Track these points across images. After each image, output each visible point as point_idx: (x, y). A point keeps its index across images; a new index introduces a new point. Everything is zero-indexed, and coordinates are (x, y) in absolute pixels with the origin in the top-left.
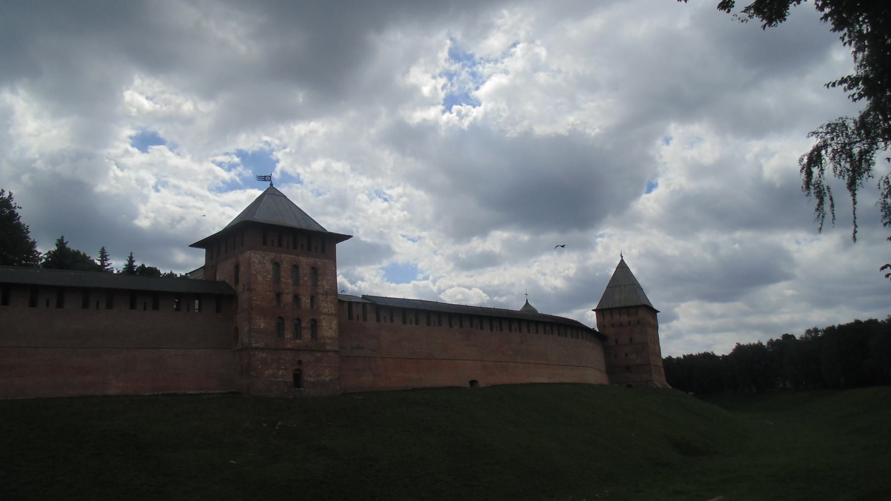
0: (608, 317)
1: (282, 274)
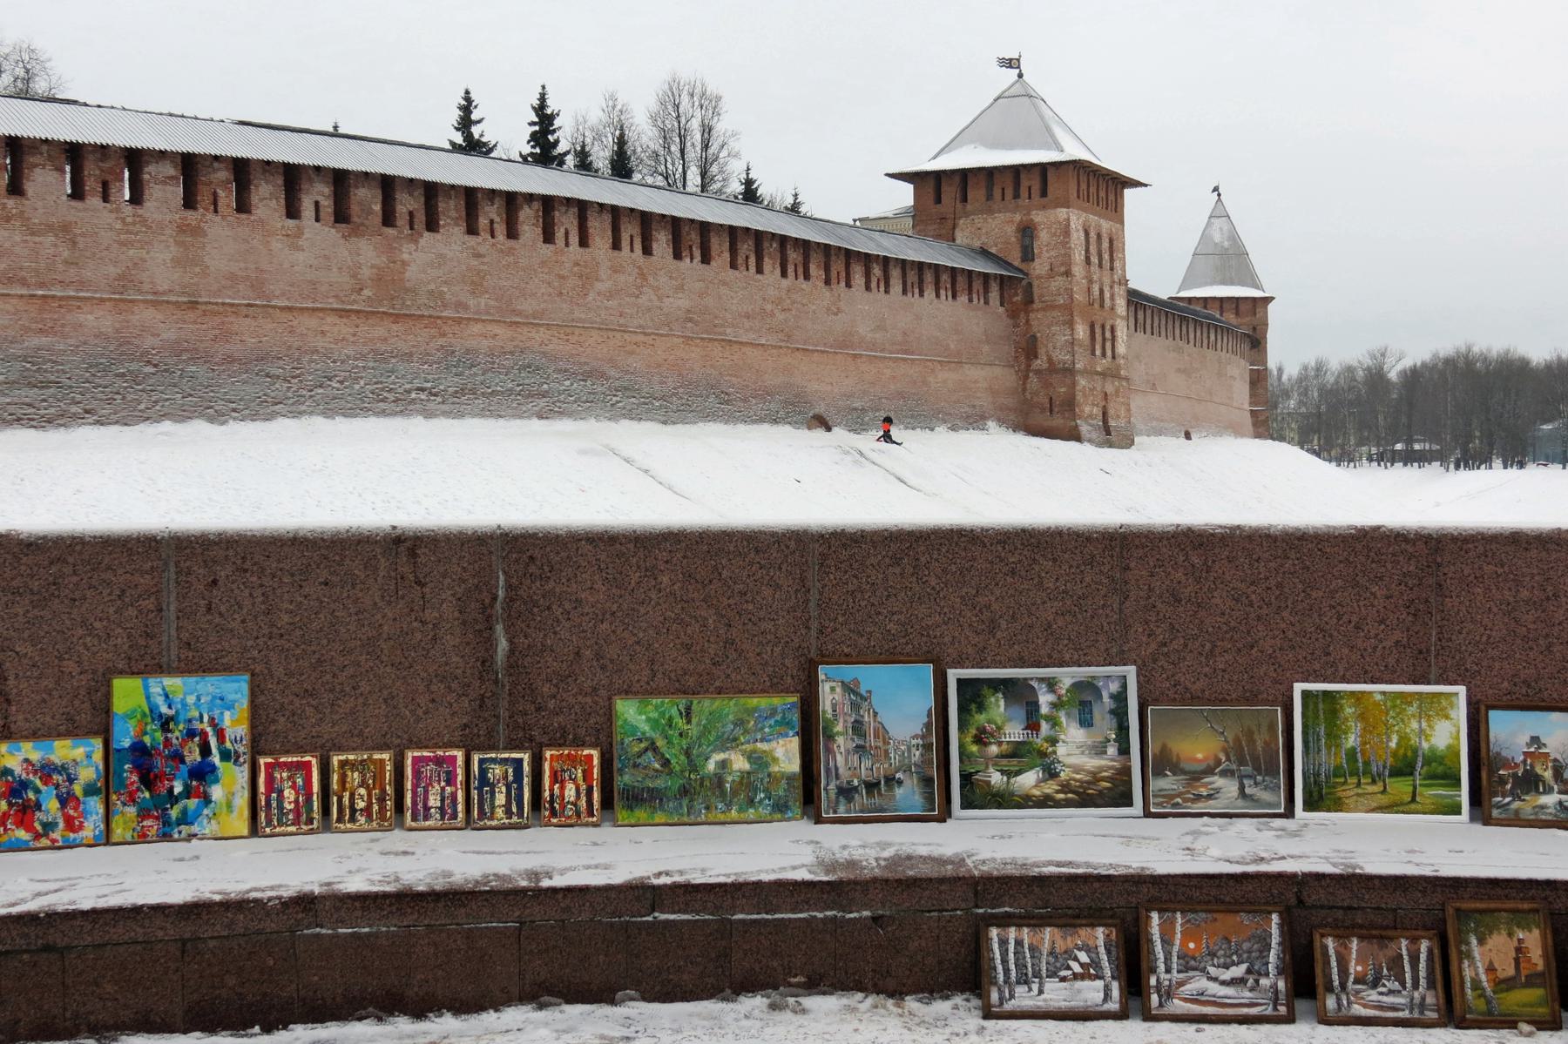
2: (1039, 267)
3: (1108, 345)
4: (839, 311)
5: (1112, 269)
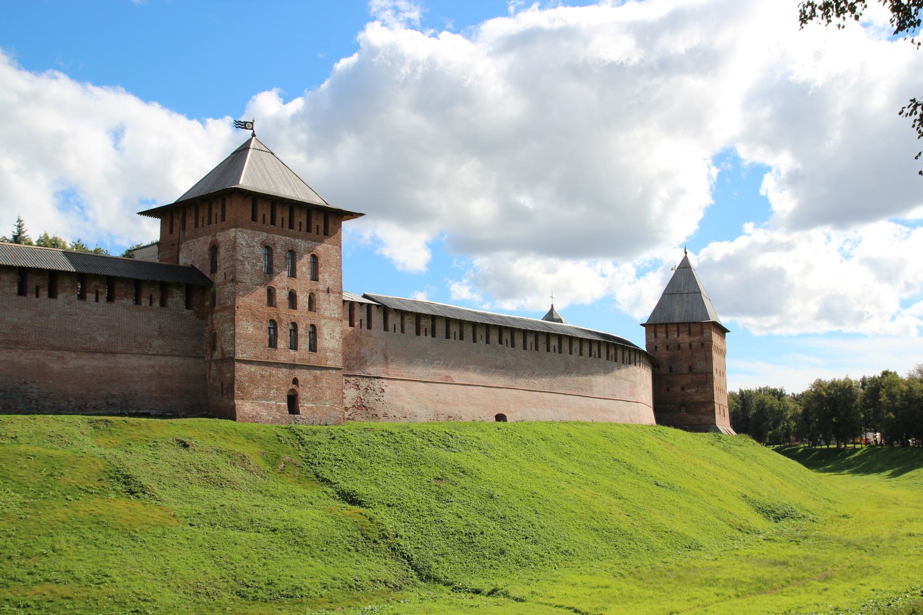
0: (662, 335)
1: (275, 261)
2: (219, 278)
5: (315, 277)
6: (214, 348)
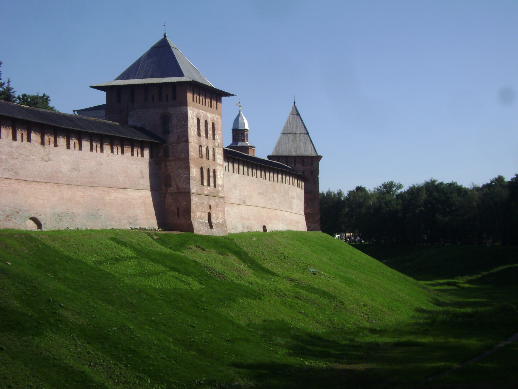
2: (172, 138)
3: (212, 180)
4: (49, 160)
5: (214, 139)
6: (168, 184)
